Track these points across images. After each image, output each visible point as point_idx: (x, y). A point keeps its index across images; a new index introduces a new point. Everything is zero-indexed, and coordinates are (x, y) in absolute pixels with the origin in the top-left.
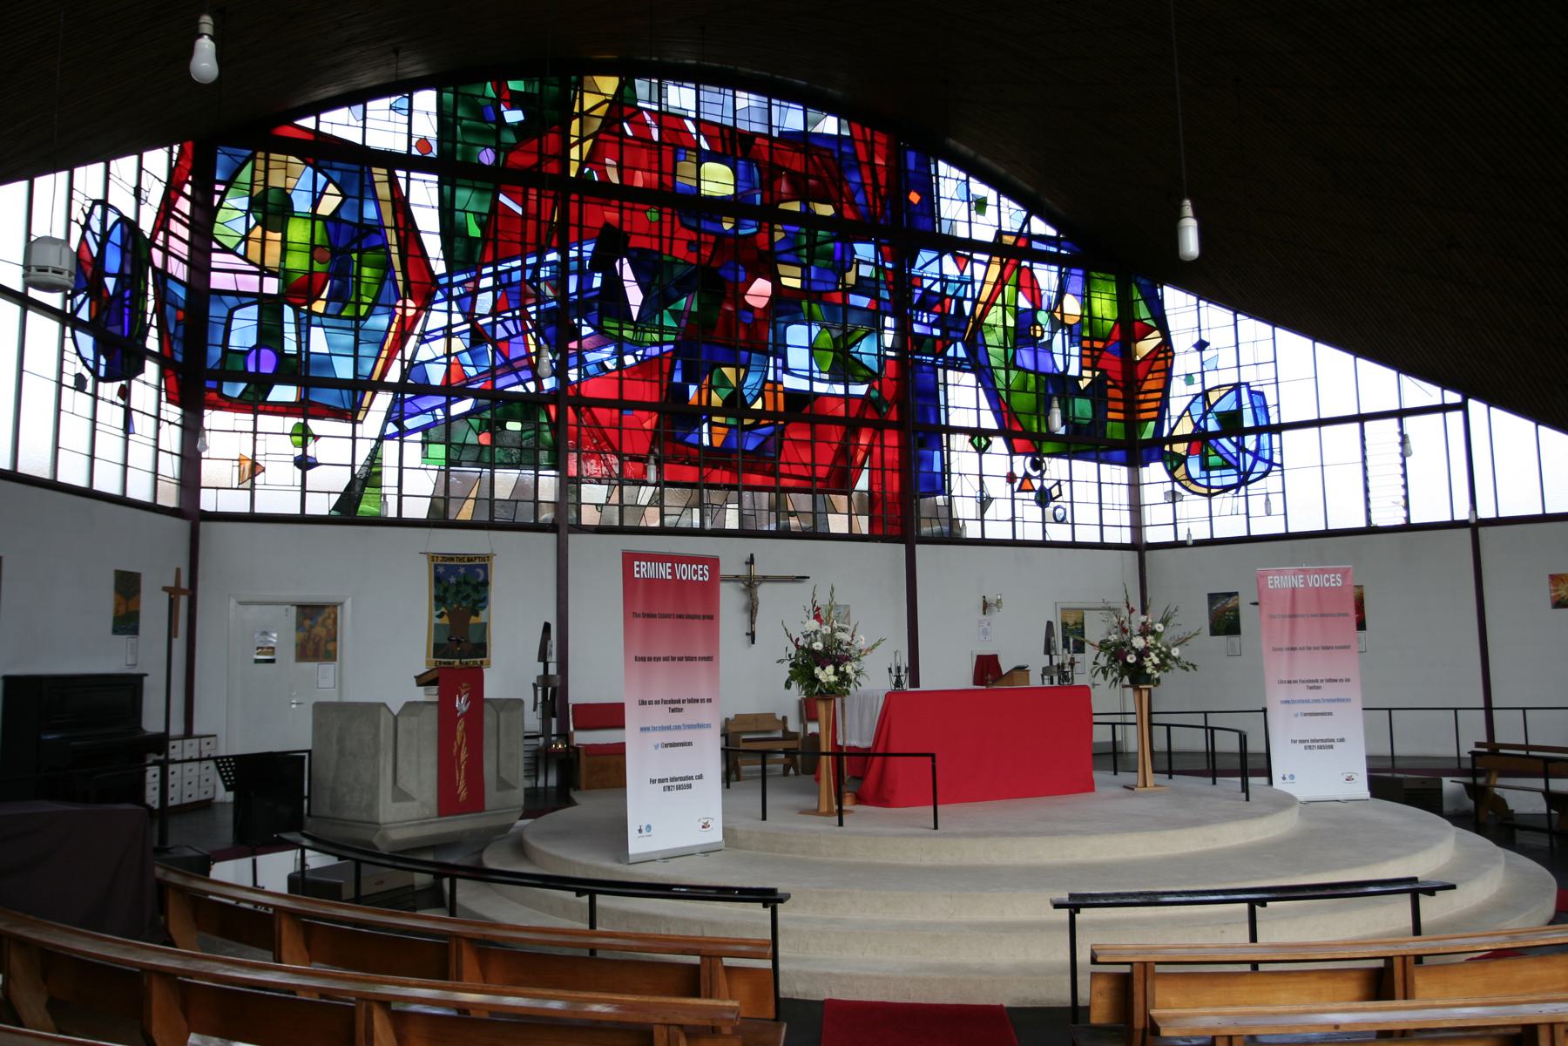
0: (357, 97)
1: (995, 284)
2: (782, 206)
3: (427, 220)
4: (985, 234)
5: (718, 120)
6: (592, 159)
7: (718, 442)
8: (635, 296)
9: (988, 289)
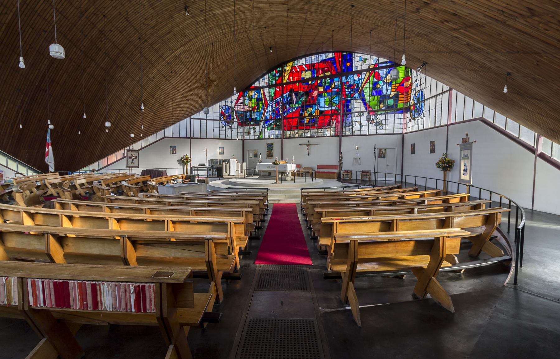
0: (258, 79)
1: (367, 78)
2: (320, 76)
3: (267, 95)
4: (366, 67)
5: (309, 63)
6: (289, 78)
7: (307, 122)
8: (295, 99)
9: (365, 80)
